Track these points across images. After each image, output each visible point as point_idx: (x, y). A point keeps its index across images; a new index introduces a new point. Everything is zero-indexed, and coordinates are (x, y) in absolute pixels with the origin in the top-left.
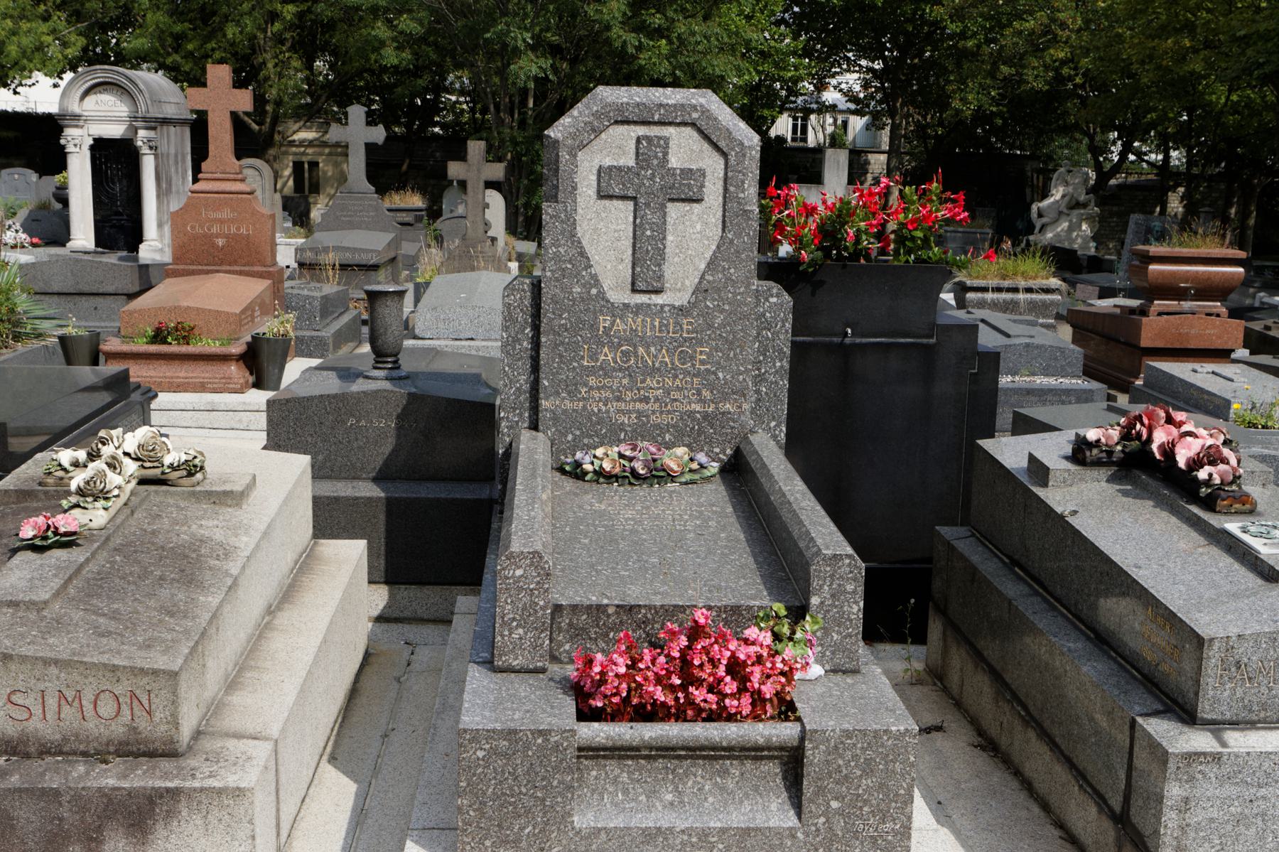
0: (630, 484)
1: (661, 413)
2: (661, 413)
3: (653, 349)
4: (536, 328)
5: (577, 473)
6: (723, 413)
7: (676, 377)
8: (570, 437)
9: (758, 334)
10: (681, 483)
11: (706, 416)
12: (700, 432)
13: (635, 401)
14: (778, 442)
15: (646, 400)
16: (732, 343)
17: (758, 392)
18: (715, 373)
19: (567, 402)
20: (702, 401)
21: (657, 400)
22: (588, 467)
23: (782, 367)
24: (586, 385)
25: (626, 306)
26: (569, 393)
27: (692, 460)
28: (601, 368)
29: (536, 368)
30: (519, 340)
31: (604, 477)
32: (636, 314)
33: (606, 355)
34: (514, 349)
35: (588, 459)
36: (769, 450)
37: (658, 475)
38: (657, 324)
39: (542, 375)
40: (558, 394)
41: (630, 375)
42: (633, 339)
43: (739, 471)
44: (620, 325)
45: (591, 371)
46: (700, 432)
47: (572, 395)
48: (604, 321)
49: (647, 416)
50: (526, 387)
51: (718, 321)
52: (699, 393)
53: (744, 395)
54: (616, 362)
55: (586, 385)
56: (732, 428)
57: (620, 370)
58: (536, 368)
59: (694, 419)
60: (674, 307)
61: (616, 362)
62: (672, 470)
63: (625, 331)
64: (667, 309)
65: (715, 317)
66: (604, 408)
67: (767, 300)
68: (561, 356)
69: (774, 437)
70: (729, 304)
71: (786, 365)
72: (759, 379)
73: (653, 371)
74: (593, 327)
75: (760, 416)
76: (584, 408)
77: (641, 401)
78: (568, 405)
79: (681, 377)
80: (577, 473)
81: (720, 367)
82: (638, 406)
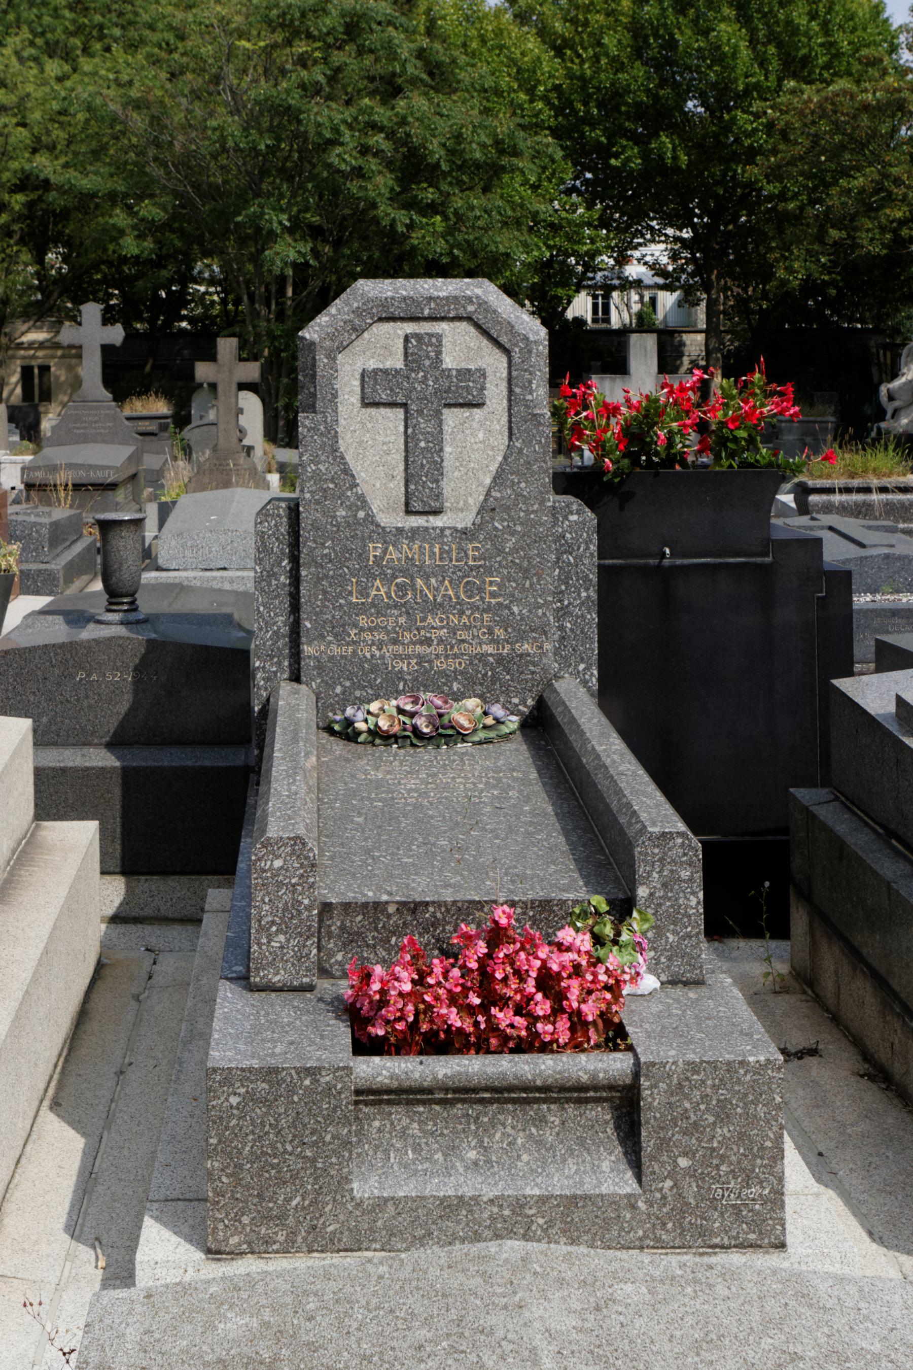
0: (413, 745)
1: (447, 657)
2: (447, 657)
3: (433, 581)
4: (295, 559)
5: (348, 733)
6: (521, 656)
7: (461, 613)
8: (338, 690)
9: (558, 559)
10: (474, 743)
11: (500, 659)
12: (494, 679)
13: (414, 644)
14: (589, 689)
15: (428, 642)
16: (527, 571)
17: (561, 628)
18: (508, 607)
19: (334, 647)
20: (495, 641)
21: (441, 641)
22: (361, 726)
23: (588, 597)
24: (355, 625)
25: (400, 530)
26: (336, 636)
27: (485, 713)
28: (373, 605)
29: (295, 607)
30: (275, 574)
31: (381, 737)
32: (412, 539)
33: (379, 589)
34: (269, 585)
35: (360, 715)
36: (579, 700)
37: (446, 734)
38: (437, 550)
39: (303, 616)
40: (323, 637)
41: (408, 613)
43: (542, 725)
44: (393, 554)
45: (362, 609)
46: (494, 679)
47: (340, 638)
48: (374, 549)
49: (430, 662)
50: (285, 630)
51: (509, 545)
52: (490, 631)
53: (545, 633)
54: (390, 597)
55: (355, 625)
56: (533, 673)
57: (396, 606)
58: (295, 607)
59: (486, 664)
60: (456, 530)
61: (390, 597)
62: (462, 727)
63: (399, 560)
64: (447, 532)
65: (505, 541)
66: (378, 653)
67: (566, 518)
68: (325, 592)
69: (584, 683)
70: (522, 524)
71: (594, 595)
72: (562, 613)
73: (435, 607)
74: (362, 556)
75: (566, 658)
76: (354, 653)
77: (421, 643)
78: (335, 650)
79: (468, 612)
80: (348, 733)
81: (514, 599)
82: (419, 649)
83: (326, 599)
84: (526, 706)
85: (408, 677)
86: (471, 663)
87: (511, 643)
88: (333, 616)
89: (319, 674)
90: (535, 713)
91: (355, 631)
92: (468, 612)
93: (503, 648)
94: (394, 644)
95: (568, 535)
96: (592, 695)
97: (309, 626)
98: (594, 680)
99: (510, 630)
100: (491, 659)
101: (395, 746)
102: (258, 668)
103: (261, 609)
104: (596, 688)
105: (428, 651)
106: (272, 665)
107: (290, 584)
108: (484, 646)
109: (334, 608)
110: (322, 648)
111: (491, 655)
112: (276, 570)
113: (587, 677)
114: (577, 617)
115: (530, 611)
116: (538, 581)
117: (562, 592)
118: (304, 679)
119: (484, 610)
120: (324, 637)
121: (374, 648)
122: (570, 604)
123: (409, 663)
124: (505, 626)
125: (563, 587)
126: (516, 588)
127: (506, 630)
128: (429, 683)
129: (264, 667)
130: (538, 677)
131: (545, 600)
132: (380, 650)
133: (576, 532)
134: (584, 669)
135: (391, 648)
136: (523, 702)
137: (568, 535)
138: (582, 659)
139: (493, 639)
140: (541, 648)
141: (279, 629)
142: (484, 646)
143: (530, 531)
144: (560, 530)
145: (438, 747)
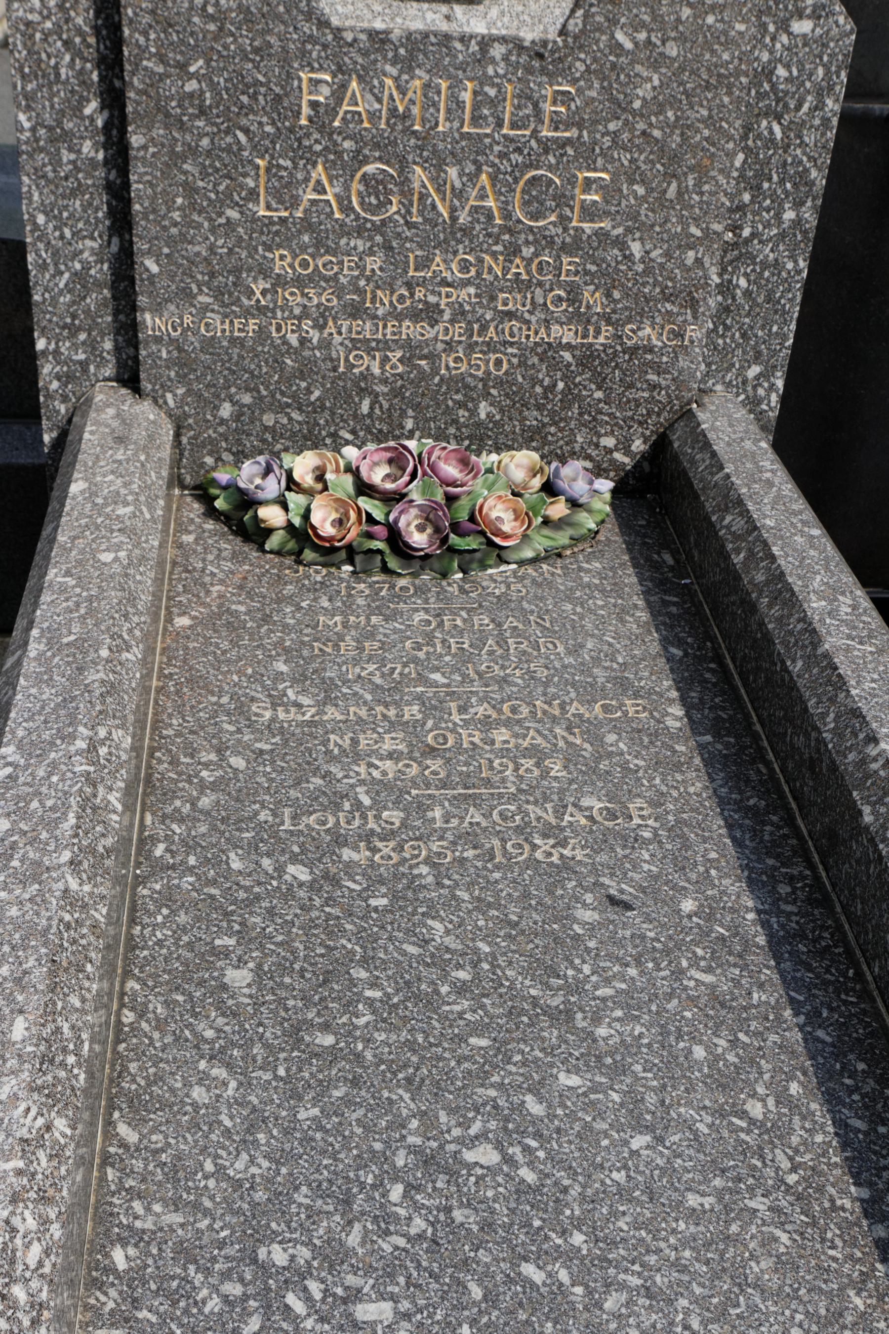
0: (385, 569)
1: (471, 347)
2: (471, 347)
3: (453, 172)
4: (114, 99)
5: (240, 518)
6: (633, 351)
7: (513, 251)
8: (226, 410)
9: (748, 129)
10: (521, 563)
11: (587, 358)
12: (570, 397)
13: (400, 317)
14: (760, 416)
15: (431, 313)
16: (675, 158)
17: (726, 288)
18: (621, 244)
19: (214, 319)
20: (581, 318)
21: (459, 313)
22: (272, 515)
23: (798, 222)
24: (264, 272)
25: (379, 39)
26: (218, 293)
27: (550, 489)
28: (307, 225)
29: (121, 220)
30: (67, 136)
31: (316, 548)
32: (408, 65)
33: (321, 189)
34: (56, 162)
35: (272, 487)
36: (739, 441)
37: (464, 543)
38: (467, 97)
39: (140, 245)
40: (190, 296)
41: (388, 247)
42: (403, 140)
43: (664, 503)
44: (359, 101)
45: (279, 234)
46: (570, 397)
47: (228, 298)
48: (313, 87)
49: (432, 357)
50: (101, 271)
51: (644, 91)
52: (573, 295)
53: (693, 304)
54: (347, 209)
55: (264, 272)
56: (653, 387)
57: (360, 231)
58: (121, 220)
59: (555, 365)
60: (518, 45)
61: (347, 209)
62: (499, 533)
63: (374, 116)
64: (497, 51)
65: (635, 80)
66: (315, 336)
67: (784, 26)
68: (190, 190)
69: (753, 404)
70: (682, 39)
71: (810, 217)
72: (736, 254)
73: (454, 235)
74: (282, 104)
75: (725, 352)
76: (262, 333)
77: (415, 316)
78: (217, 325)
79: (527, 252)
80: (240, 518)
81: (636, 225)
82: (408, 329)
83: (193, 206)
84: (627, 452)
85: (381, 389)
86: (523, 364)
87: (615, 324)
88: (212, 249)
89: (182, 378)
90: (646, 466)
91: (263, 284)
92: (527, 252)
93: (598, 332)
94: (354, 316)
95: (781, 72)
96: (763, 428)
97: (155, 269)
98: (774, 398)
99: (616, 295)
100: (567, 356)
101: (349, 568)
102: (44, 352)
103: (41, 219)
104: (773, 415)
105: (430, 333)
106: (75, 347)
107: (106, 162)
108: (555, 328)
109: (213, 230)
110: (188, 320)
111: (569, 347)
112: (69, 125)
113: (761, 392)
114: (765, 265)
115: (668, 255)
116: (699, 184)
117: (741, 208)
118: (146, 386)
119: (564, 248)
120: (192, 296)
121: (307, 324)
122: (753, 235)
123: (385, 360)
124: (608, 281)
125: (747, 197)
126: (644, 199)
127: (608, 295)
128: (426, 401)
129: (57, 352)
130: (662, 397)
131: (706, 231)
132: (322, 328)
133: (801, 65)
134: (757, 378)
135: (345, 325)
136: (625, 446)
137: (781, 72)
138: (757, 357)
139: (577, 313)
140: (680, 335)
141: (86, 267)
142: (555, 328)
143: (698, 58)
144: (765, 57)
145: (444, 575)
